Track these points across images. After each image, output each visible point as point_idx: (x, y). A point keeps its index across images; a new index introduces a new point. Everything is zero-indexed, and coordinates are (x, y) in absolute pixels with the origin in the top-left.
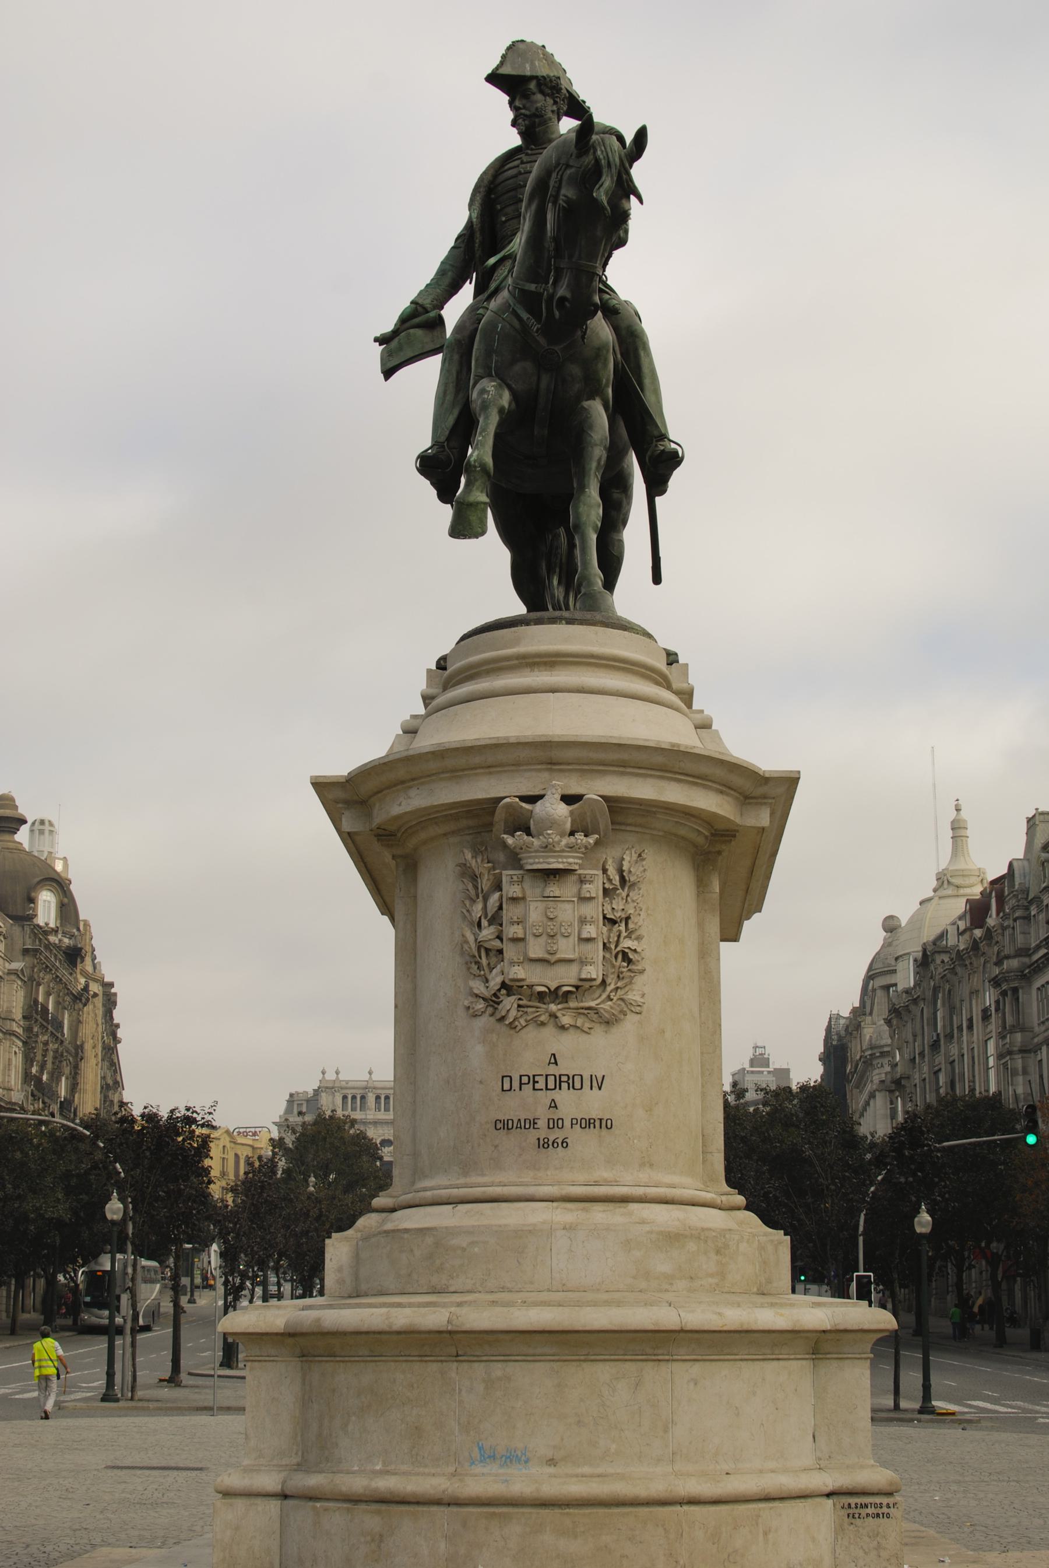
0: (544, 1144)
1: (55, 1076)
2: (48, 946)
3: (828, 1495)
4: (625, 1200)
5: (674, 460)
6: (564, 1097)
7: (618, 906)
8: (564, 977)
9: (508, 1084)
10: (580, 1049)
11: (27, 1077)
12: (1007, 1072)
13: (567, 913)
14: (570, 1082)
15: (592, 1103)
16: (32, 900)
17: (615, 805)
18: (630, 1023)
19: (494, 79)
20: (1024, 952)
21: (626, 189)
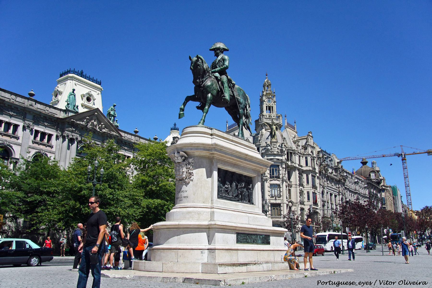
0: (180, 200)
2: (373, 182)
3: (208, 249)
4: (187, 207)
6: (182, 193)
15: (185, 194)
16: (370, 175)
19: (211, 50)
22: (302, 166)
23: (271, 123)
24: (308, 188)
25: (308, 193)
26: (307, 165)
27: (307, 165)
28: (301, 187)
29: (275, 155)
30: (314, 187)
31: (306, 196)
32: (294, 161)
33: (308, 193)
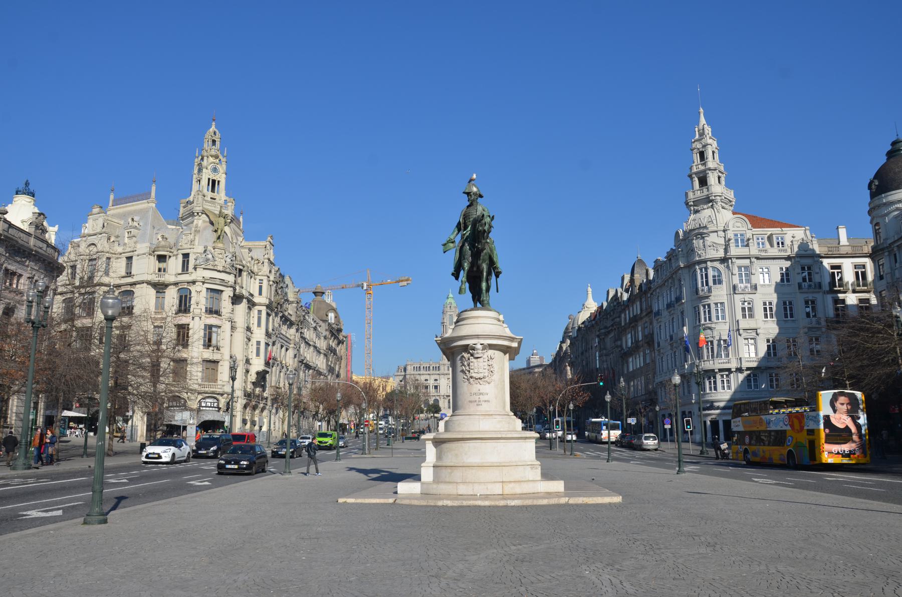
1: (335, 364)
5: (500, 273)
6: (481, 396)
7: (490, 363)
8: (481, 375)
9: (471, 394)
10: (484, 388)
11: (327, 365)
12: (601, 362)
13: (481, 364)
14: (482, 394)
17: (489, 345)
18: (492, 384)
20: (606, 328)
21: (490, 227)
22: (252, 295)
23: (218, 213)
24: (259, 334)
25: (258, 343)
26: (260, 294)
27: (260, 294)
28: (249, 333)
29: (219, 271)
30: (268, 335)
31: (254, 349)
32: (244, 286)
33: (258, 343)
